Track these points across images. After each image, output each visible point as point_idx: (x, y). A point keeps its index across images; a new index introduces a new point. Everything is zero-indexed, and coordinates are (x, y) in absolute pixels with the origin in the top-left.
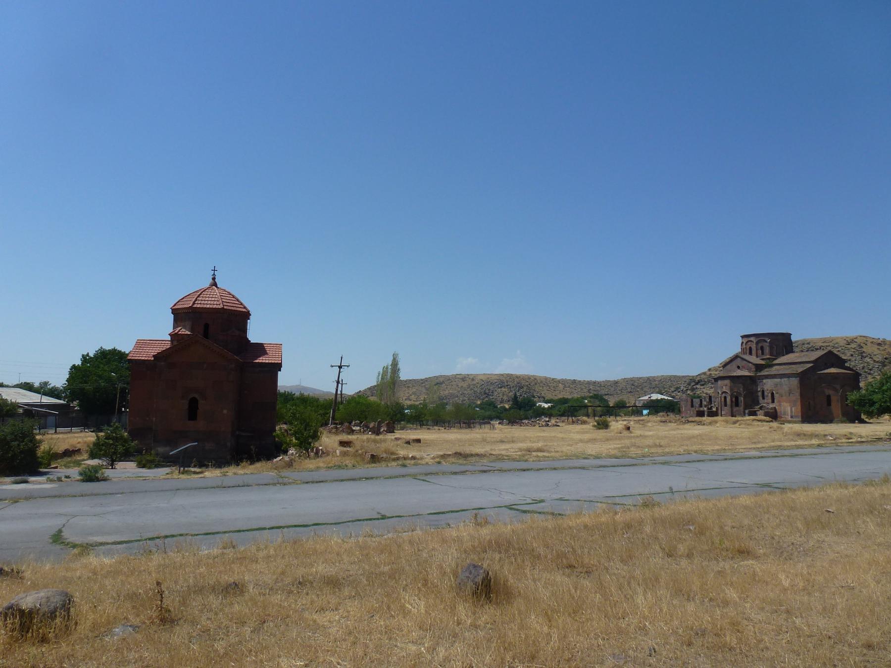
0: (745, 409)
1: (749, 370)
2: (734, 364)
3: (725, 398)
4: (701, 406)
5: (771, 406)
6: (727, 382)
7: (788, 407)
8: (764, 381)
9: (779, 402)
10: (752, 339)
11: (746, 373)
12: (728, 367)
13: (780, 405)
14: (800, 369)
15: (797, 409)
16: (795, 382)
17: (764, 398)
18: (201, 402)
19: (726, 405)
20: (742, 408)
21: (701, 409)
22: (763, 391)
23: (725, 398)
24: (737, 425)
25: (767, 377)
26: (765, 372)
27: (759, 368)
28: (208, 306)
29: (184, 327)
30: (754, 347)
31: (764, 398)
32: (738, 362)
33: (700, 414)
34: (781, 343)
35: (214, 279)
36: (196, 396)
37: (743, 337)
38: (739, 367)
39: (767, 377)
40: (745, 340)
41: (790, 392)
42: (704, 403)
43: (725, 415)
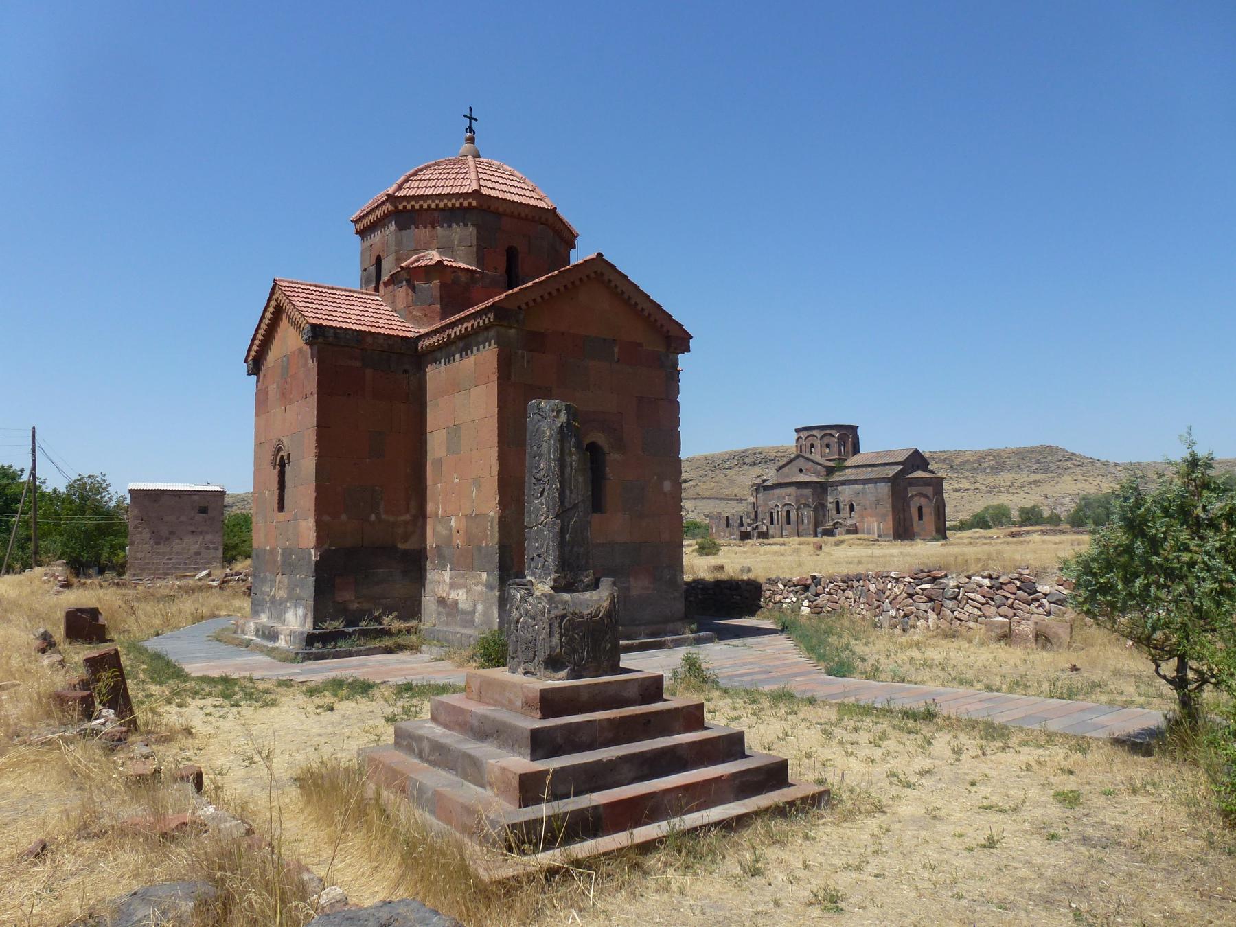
0: (816, 527)
1: (817, 474)
2: (793, 468)
3: (788, 512)
4: (741, 525)
5: (849, 522)
6: (792, 490)
7: (877, 522)
8: (840, 488)
9: (862, 516)
10: (814, 432)
11: (813, 478)
12: (785, 470)
13: (862, 521)
14: (892, 472)
15: (888, 525)
16: (884, 489)
17: (838, 512)
18: (614, 457)
19: (789, 522)
20: (811, 526)
21: (743, 529)
22: (837, 503)
23: (788, 512)
24: (843, 546)
25: (843, 483)
26: (837, 477)
27: (830, 471)
28: (517, 199)
29: (445, 249)
30: (817, 443)
31: (838, 512)
32: (801, 463)
33: (745, 536)
34: (848, 437)
35: (471, 140)
36: (600, 439)
37: (797, 431)
38: (801, 471)
39: (843, 483)
40: (803, 435)
41: (878, 503)
42: (746, 521)
43: (788, 536)
